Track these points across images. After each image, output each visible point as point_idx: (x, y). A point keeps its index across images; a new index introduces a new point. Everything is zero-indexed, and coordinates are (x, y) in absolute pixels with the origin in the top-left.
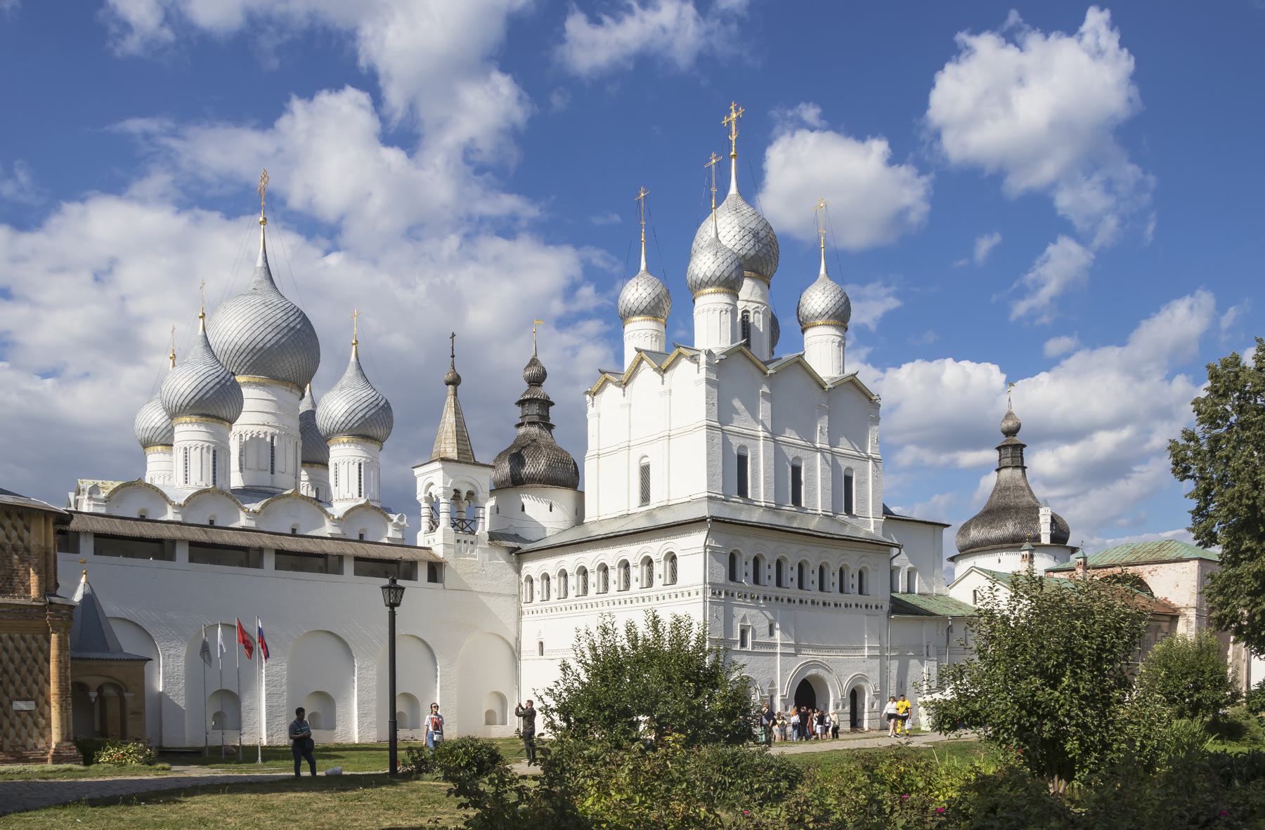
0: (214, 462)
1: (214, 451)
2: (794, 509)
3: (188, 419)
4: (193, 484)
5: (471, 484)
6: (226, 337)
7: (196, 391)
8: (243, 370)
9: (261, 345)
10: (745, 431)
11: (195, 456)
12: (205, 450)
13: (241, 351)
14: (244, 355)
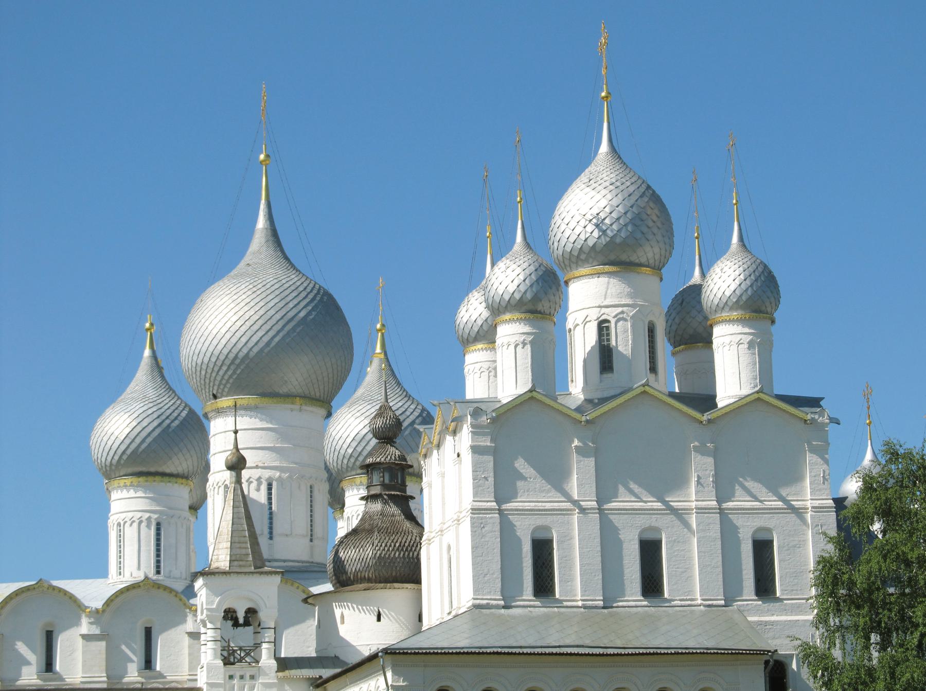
0: (158, 540)
1: (158, 524)
2: (645, 603)
3: (122, 482)
4: (127, 574)
5: (251, 600)
6: (199, 346)
7: (128, 441)
8: (226, 390)
9: (245, 351)
10: (548, 506)
11: (130, 533)
12: (143, 525)
13: (219, 363)
14: (224, 368)
